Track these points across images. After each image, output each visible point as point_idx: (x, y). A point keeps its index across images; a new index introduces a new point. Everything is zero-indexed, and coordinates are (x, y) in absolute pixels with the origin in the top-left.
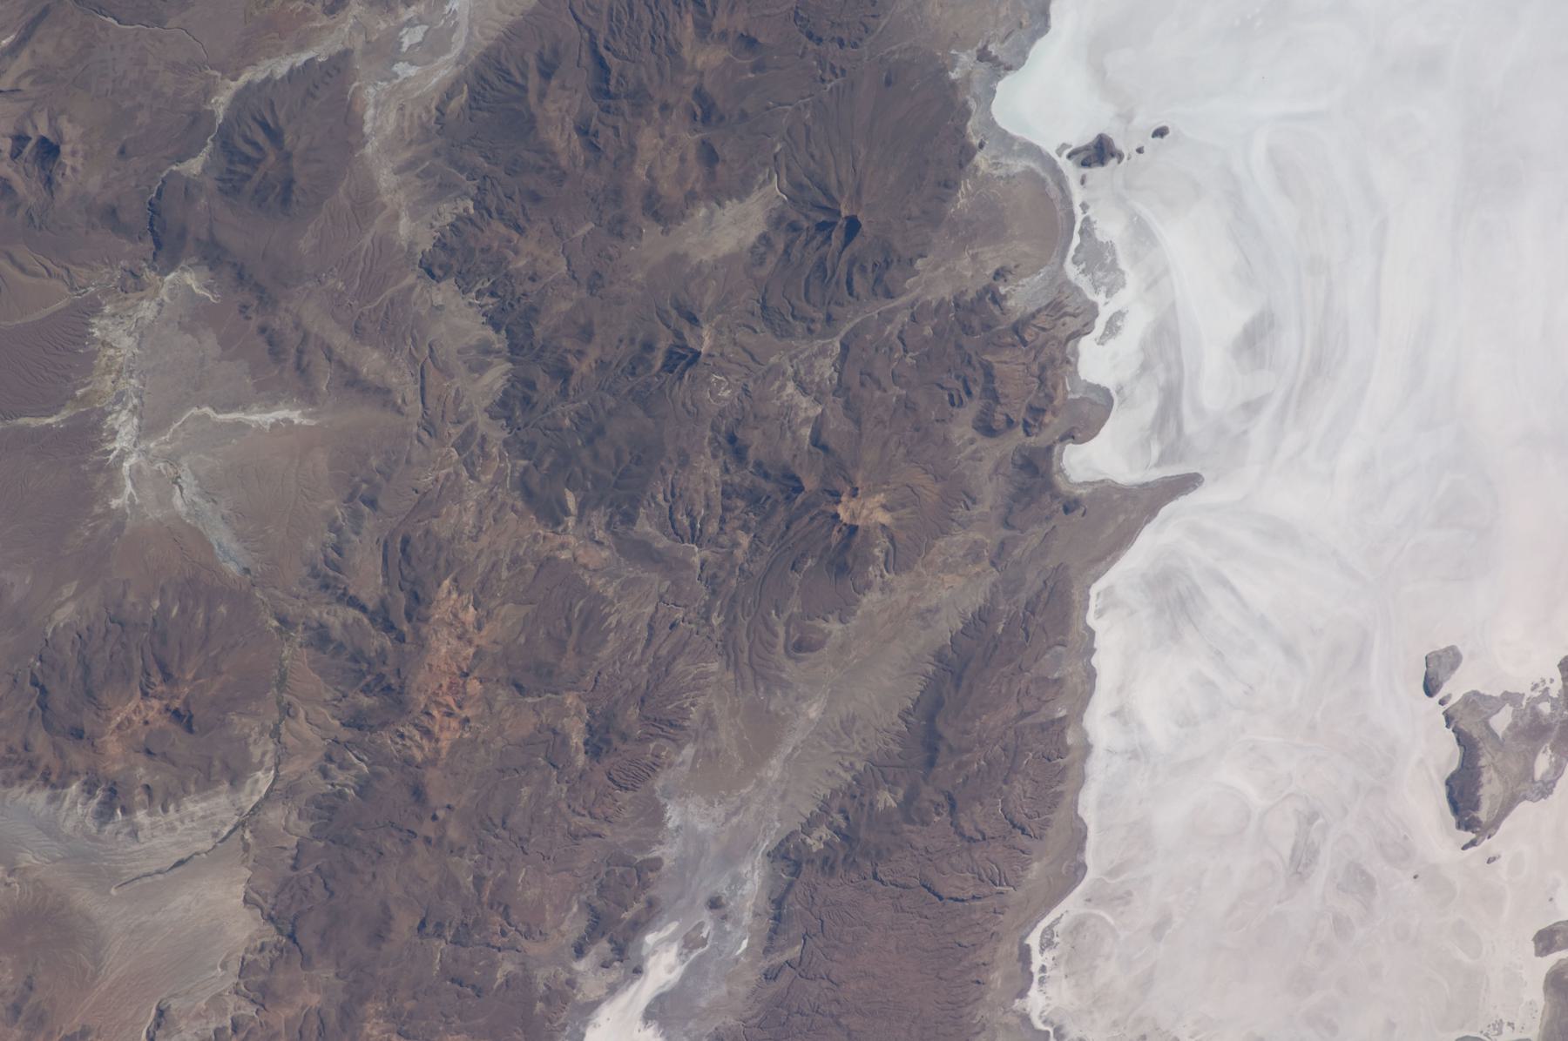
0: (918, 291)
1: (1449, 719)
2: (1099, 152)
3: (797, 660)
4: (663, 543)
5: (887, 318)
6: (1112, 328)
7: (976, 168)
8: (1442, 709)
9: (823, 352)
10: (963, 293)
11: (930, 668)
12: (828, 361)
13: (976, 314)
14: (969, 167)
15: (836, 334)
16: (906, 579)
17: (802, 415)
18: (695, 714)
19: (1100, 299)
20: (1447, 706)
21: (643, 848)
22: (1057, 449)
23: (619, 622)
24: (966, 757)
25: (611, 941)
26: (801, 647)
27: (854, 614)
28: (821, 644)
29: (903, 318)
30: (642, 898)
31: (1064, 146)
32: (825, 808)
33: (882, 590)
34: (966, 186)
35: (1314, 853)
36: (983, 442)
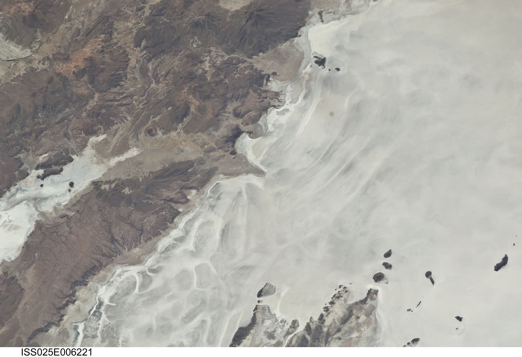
0: (254, 61)
1: (256, 309)
2: (321, 62)
3: (146, 135)
4: (150, 74)
5: (244, 62)
6: (283, 113)
7: (293, 41)
8: (257, 304)
9: (222, 56)
10: (263, 71)
11: (167, 166)
12: (221, 60)
13: (259, 79)
14: (292, 39)
15: (229, 55)
16: (183, 135)
17: (204, 67)
18: (115, 127)
19: (287, 102)
20: (259, 304)
21: (73, 153)
22: (244, 134)
23: (123, 85)
24: (151, 196)
25: (45, 172)
26: (150, 132)
27: (166, 134)
28: (153, 135)
29: (246, 64)
30: (61, 166)
31: (316, 53)
32: (114, 181)
33: (178, 133)
34: (288, 43)
35: (195, 316)
36: (231, 116)
